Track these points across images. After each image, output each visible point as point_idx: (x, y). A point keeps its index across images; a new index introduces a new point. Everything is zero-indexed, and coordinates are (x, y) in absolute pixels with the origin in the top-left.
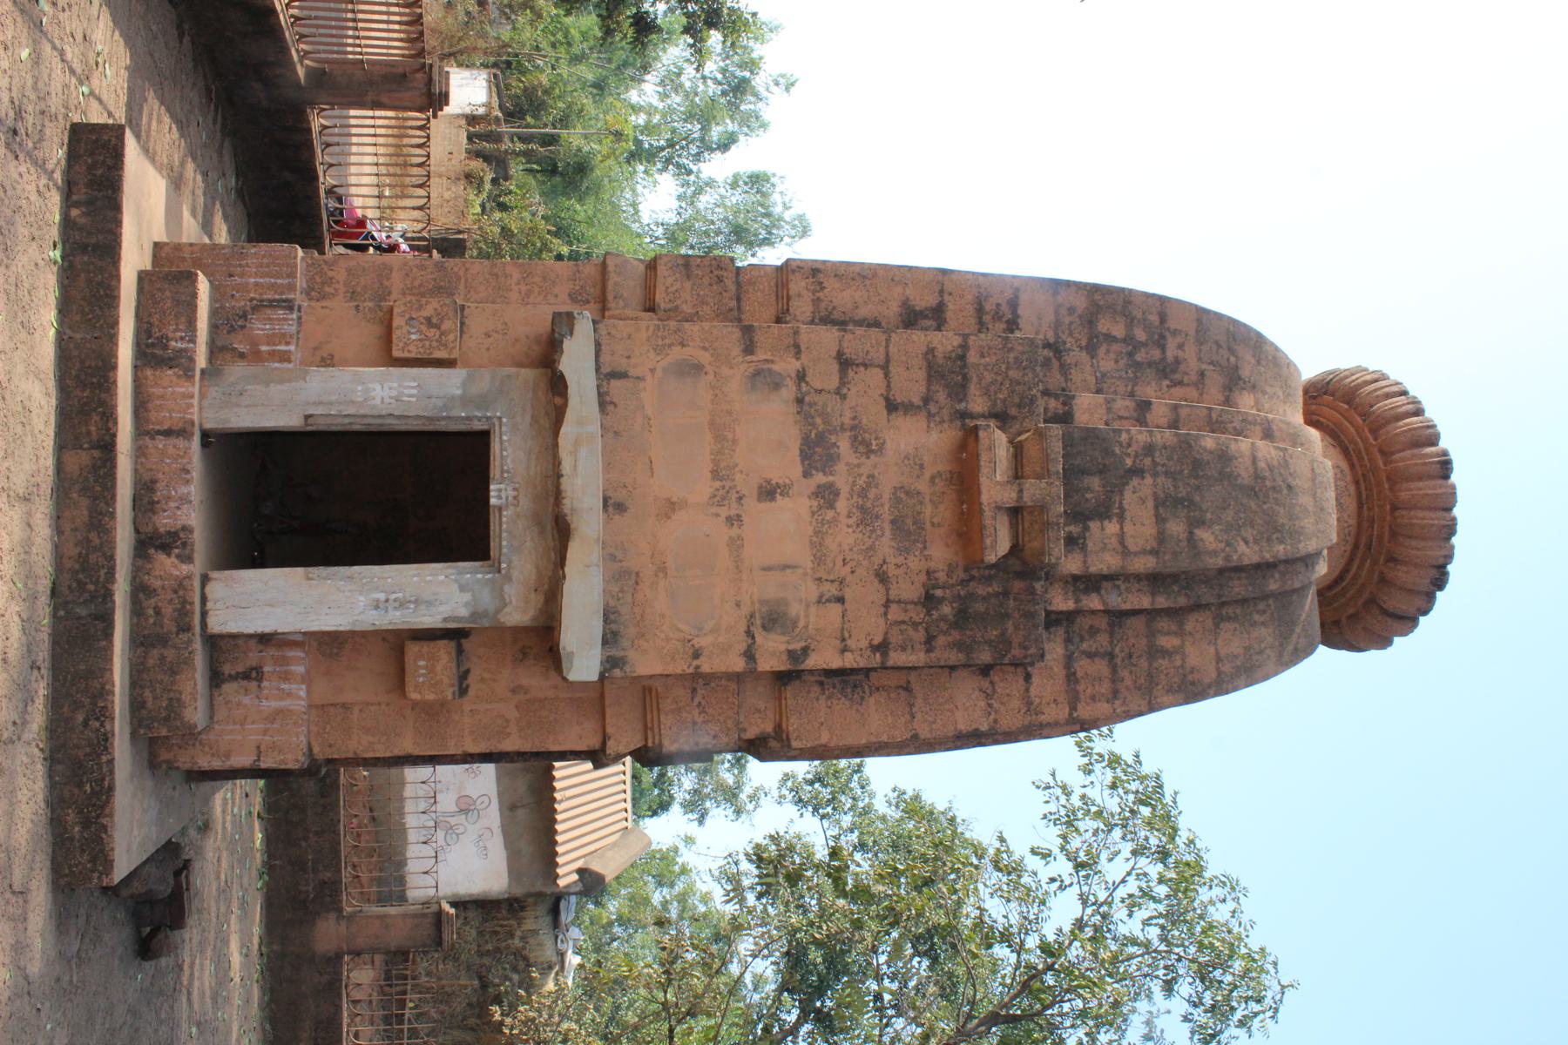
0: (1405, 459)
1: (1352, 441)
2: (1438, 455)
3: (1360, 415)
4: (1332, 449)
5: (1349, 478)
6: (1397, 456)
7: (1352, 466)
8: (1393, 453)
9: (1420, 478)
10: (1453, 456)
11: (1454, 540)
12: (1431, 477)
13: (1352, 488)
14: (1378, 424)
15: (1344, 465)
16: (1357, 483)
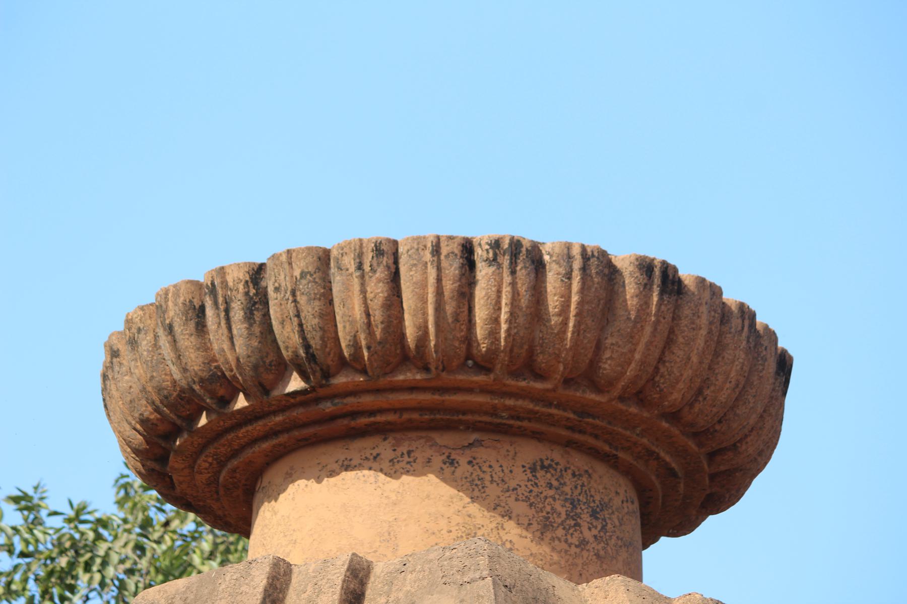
0: (623, 359)
1: (494, 411)
2: (647, 287)
3: (463, 366)
4: (482, 454)
5: (556, 455)
6: (607, 367)
7: (537, 436)
8: (594, 364)
9: (669, 342)
10: (658, 254)
11: (760, 319)
12: (676, 318)
13: (579, 461)
14: (525, 356)
15: (530, 452)
16: (569, 444)
